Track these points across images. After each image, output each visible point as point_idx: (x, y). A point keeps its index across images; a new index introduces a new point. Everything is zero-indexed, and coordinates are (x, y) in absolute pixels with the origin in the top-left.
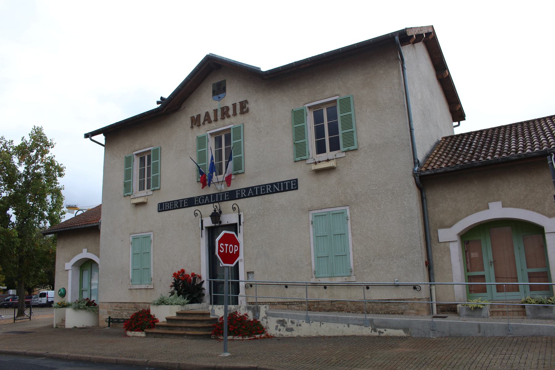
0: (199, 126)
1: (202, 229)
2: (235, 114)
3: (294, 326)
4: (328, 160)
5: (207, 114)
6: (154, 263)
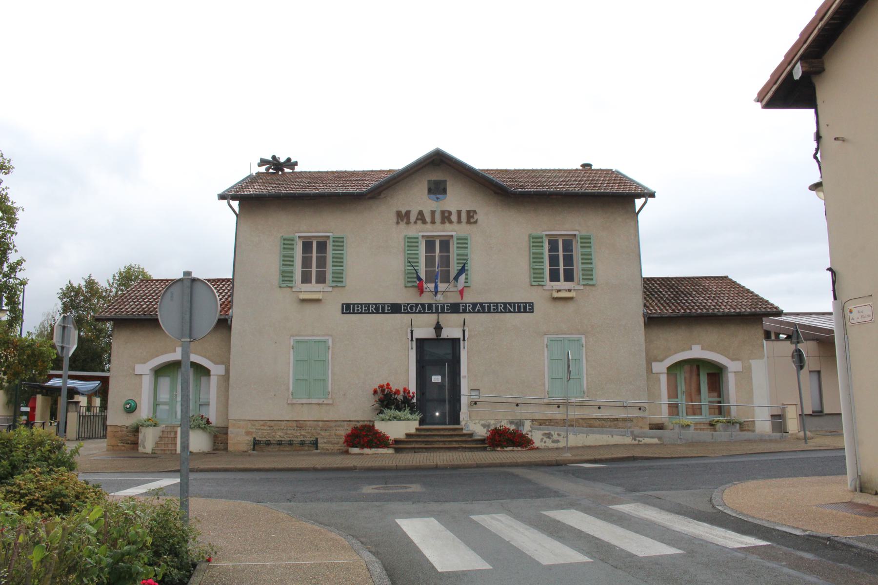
0: (408, 223)
1: (412, 340)
2: (459, 221)
3: (560, 438)
4: (570, 291)
5: (421, 213)
6: (333, 374)
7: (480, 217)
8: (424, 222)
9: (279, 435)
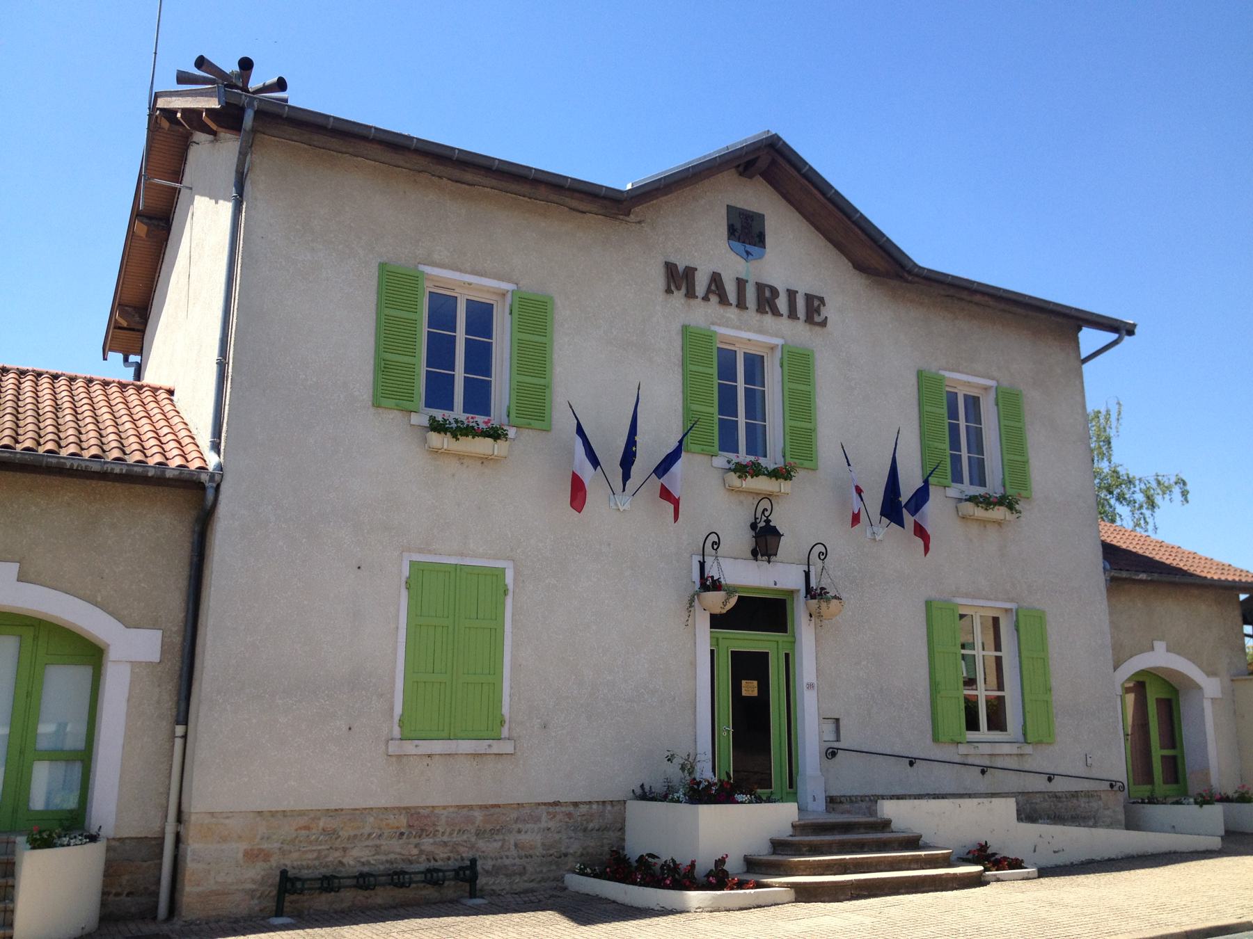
0: (690, 294)
5: (716, 279)
7: (828, 311)
8: (723, 300)
9: (357, 857)
